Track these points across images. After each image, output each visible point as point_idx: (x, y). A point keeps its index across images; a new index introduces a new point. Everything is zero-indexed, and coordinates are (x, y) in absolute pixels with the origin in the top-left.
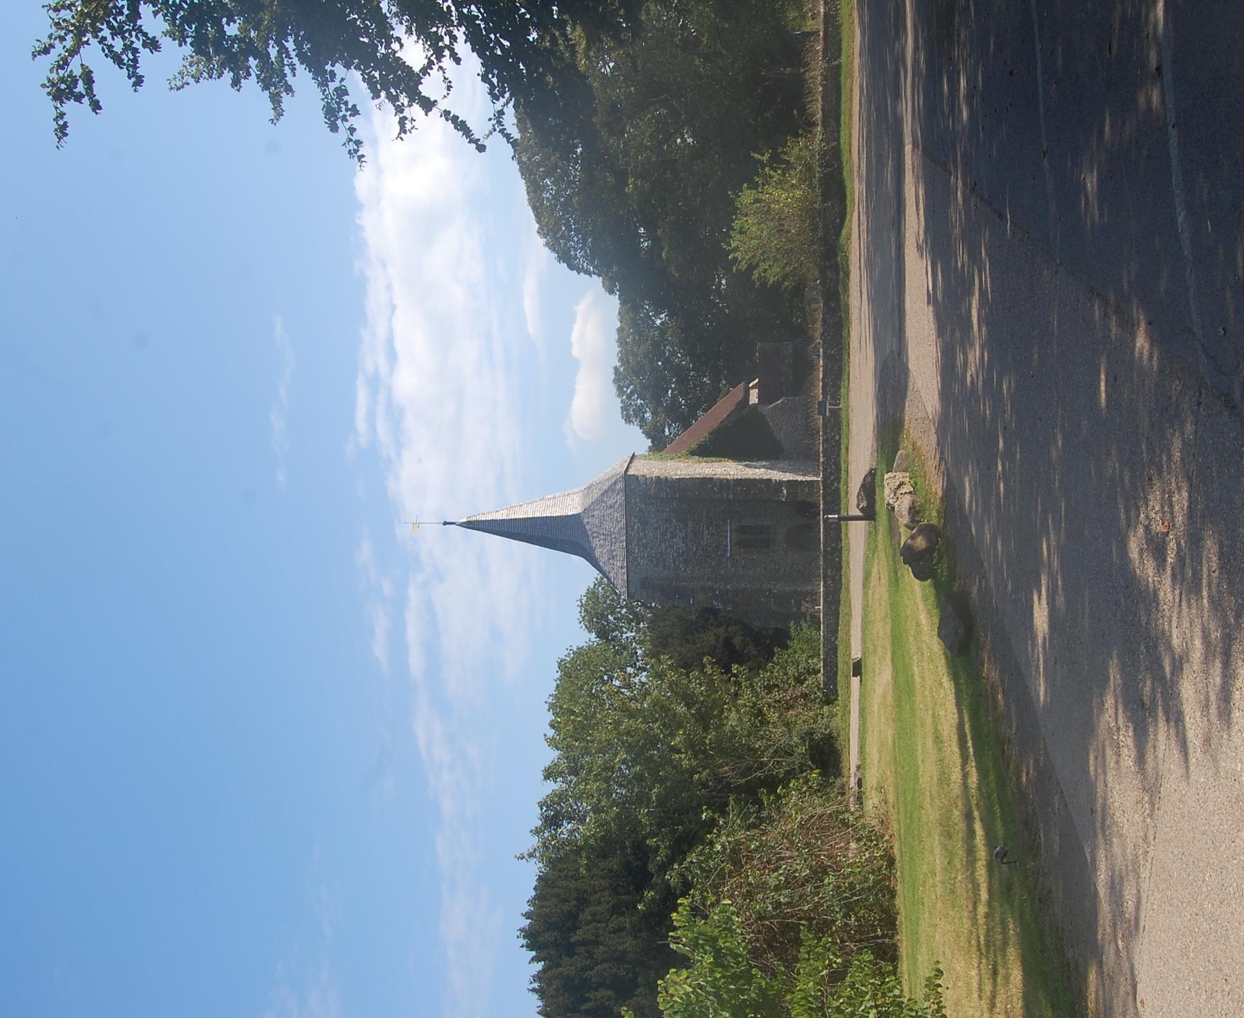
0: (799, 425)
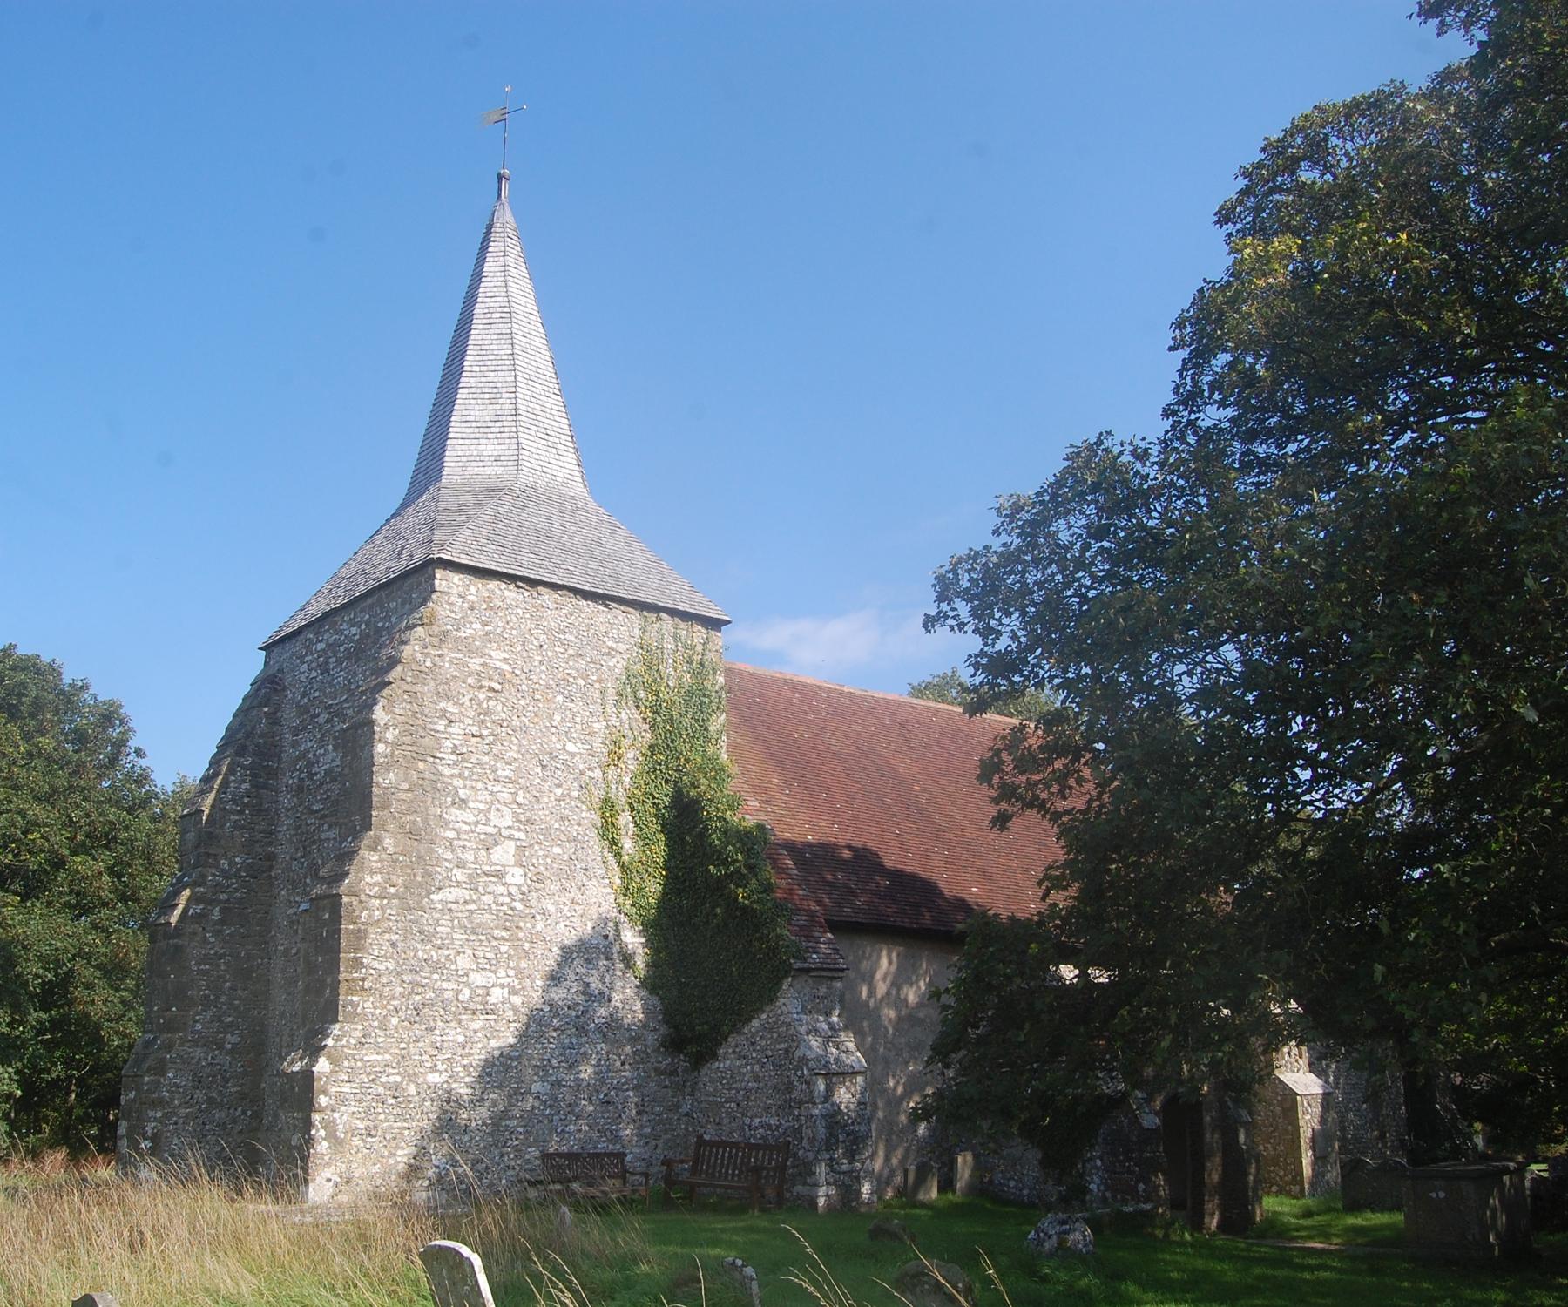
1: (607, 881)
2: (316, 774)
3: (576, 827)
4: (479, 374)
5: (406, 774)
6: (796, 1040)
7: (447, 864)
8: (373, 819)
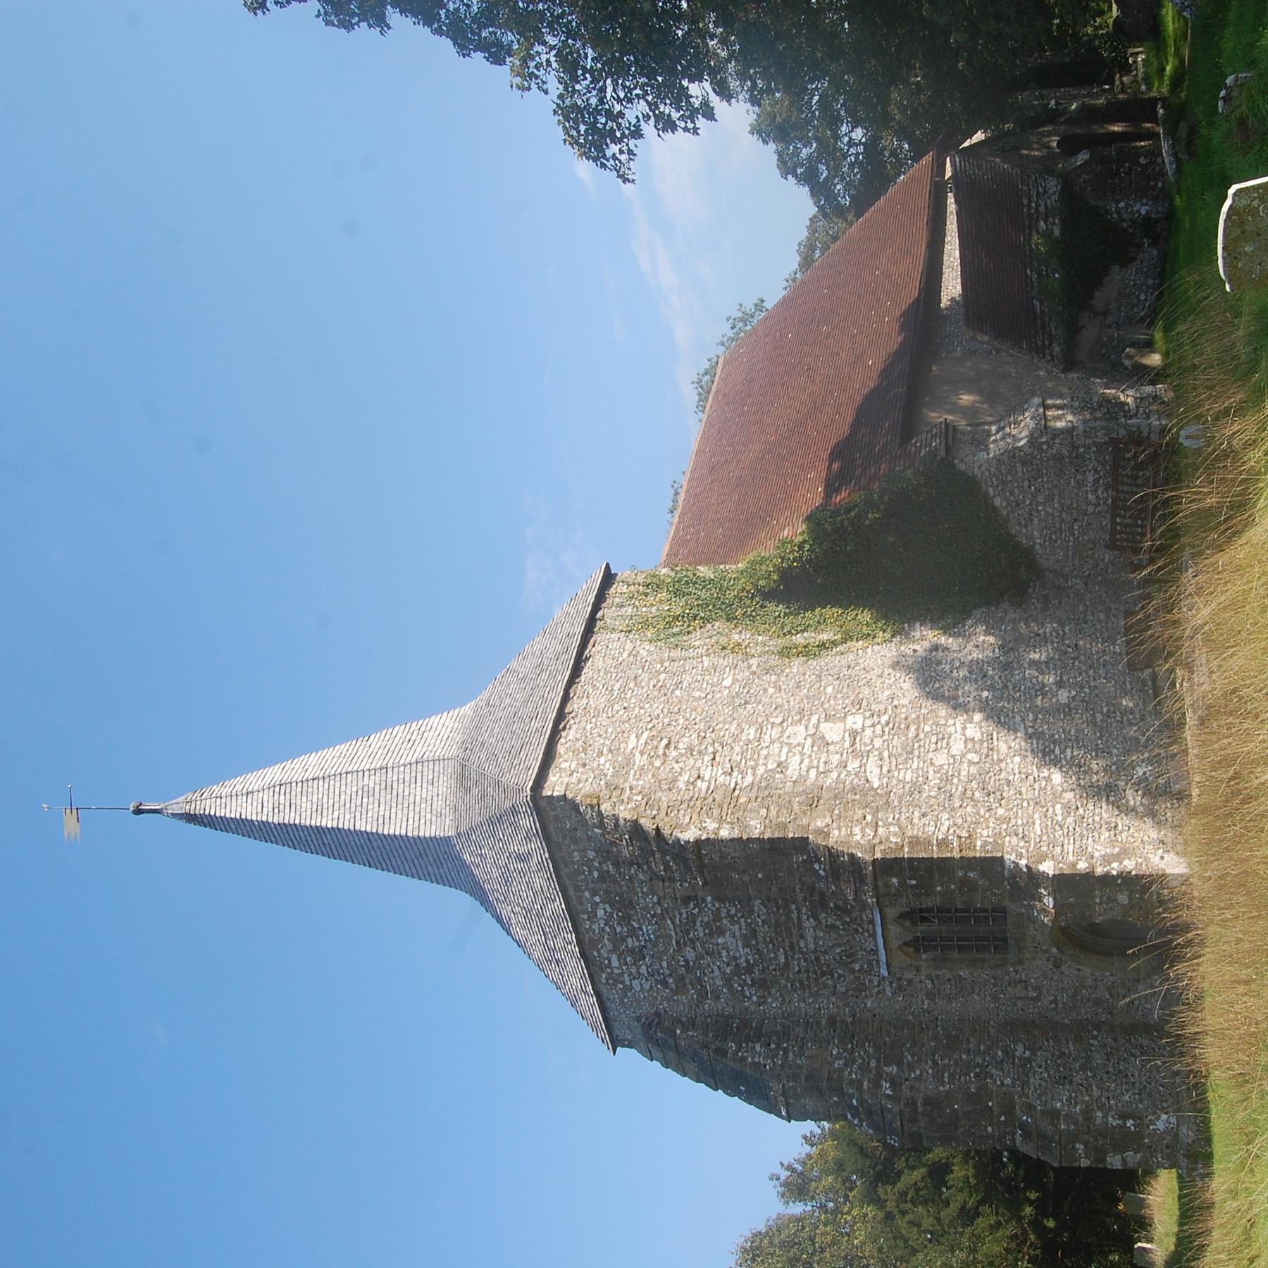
1: (860, 652)
2: (747, 961)
3: (807, 676)
4: (342, 811)
5: (751, 811)
6: (1013, 454)
7: (843, 776)
8: (796, 836)
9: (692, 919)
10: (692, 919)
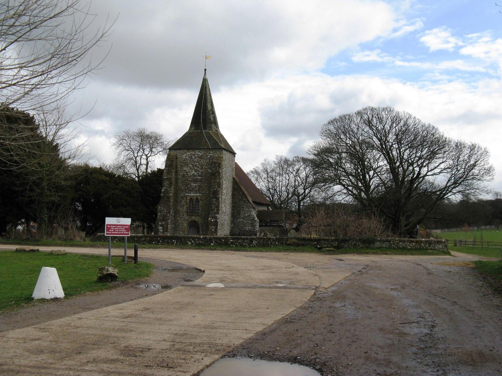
0: (246, 227)
9: (198, 167)
10: (198, 167)
